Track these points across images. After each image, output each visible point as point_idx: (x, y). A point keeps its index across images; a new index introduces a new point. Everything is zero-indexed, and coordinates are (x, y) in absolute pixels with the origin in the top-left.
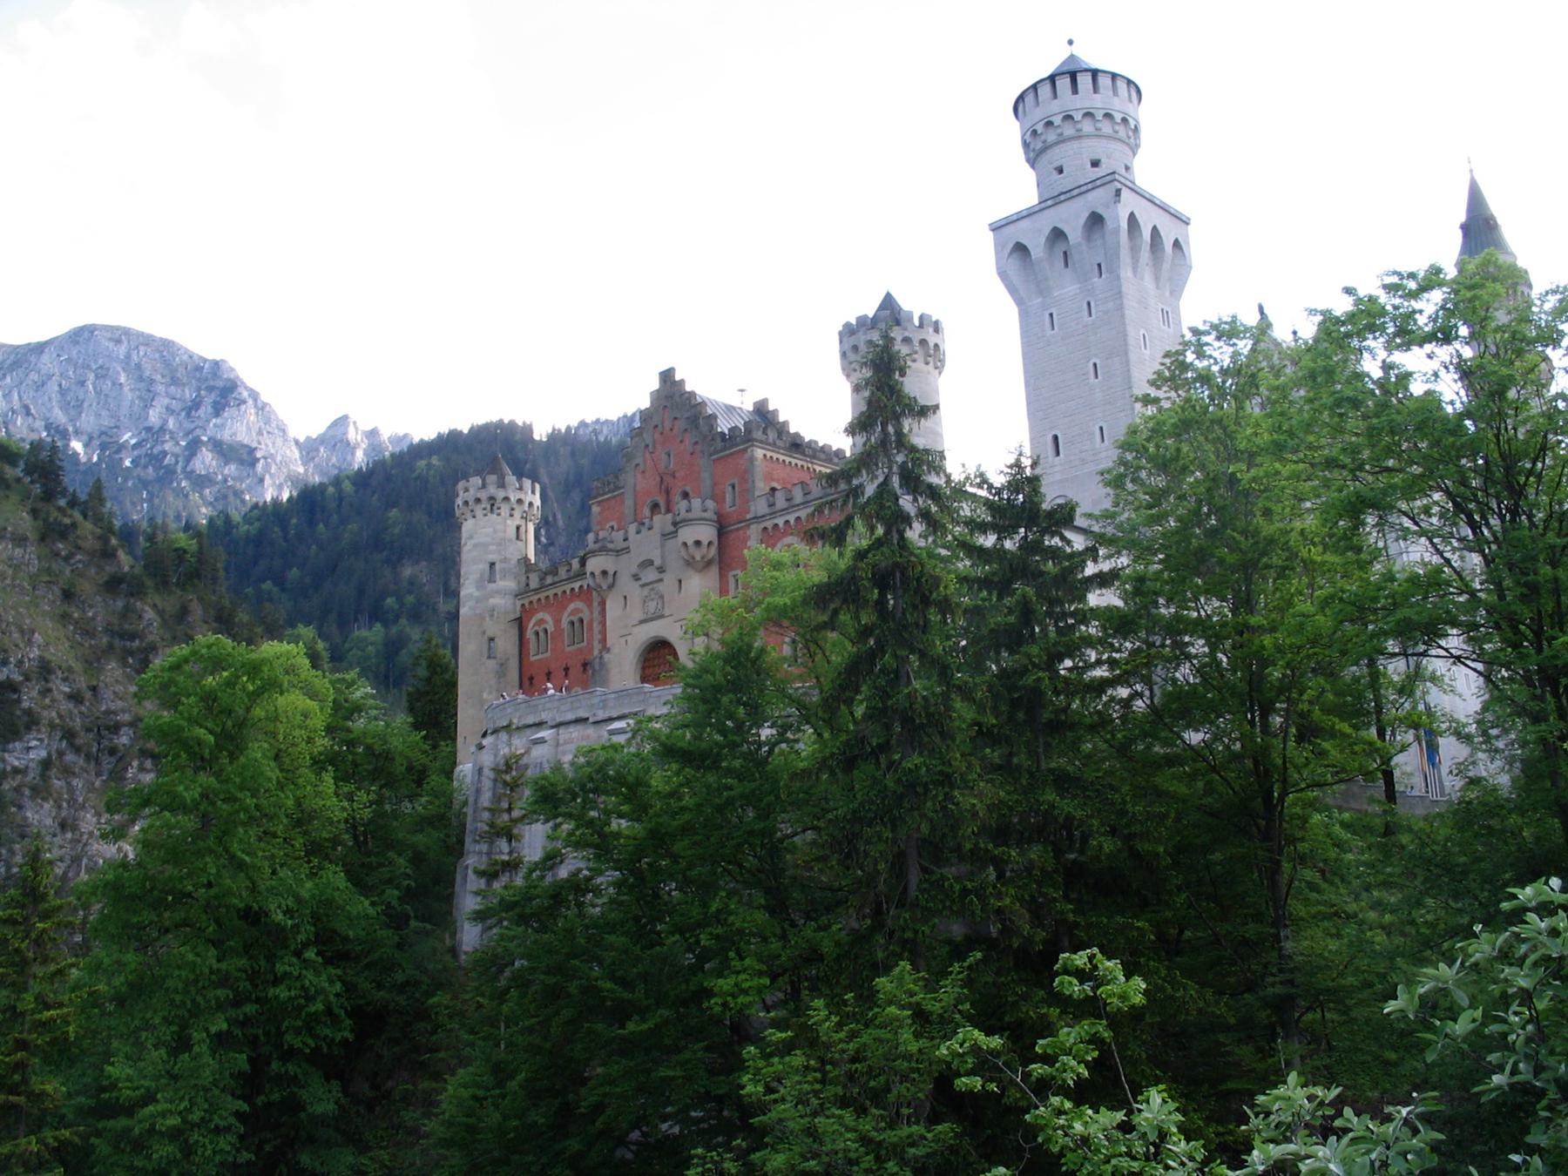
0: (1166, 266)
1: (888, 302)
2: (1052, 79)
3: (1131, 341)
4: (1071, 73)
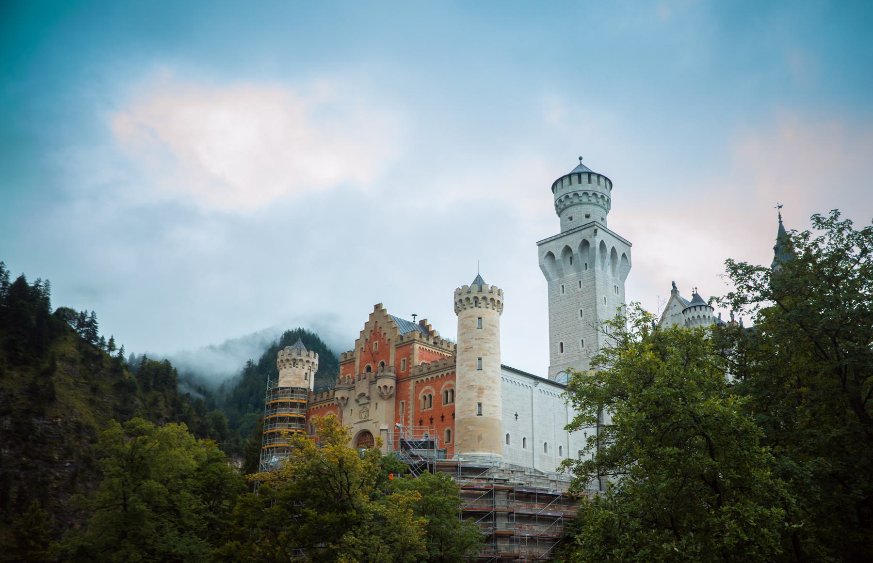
0: (618, 266)
1: (479, 281)
2: (570, 176)
3: (598, 300)
4: (581, 174)
